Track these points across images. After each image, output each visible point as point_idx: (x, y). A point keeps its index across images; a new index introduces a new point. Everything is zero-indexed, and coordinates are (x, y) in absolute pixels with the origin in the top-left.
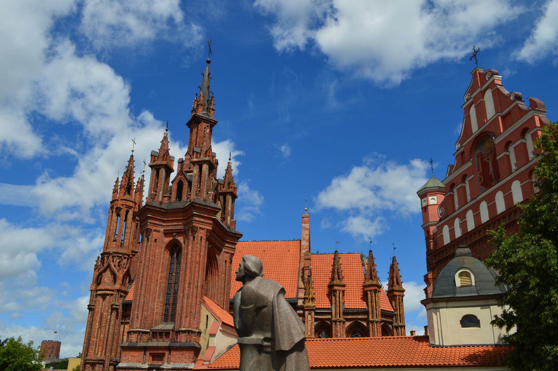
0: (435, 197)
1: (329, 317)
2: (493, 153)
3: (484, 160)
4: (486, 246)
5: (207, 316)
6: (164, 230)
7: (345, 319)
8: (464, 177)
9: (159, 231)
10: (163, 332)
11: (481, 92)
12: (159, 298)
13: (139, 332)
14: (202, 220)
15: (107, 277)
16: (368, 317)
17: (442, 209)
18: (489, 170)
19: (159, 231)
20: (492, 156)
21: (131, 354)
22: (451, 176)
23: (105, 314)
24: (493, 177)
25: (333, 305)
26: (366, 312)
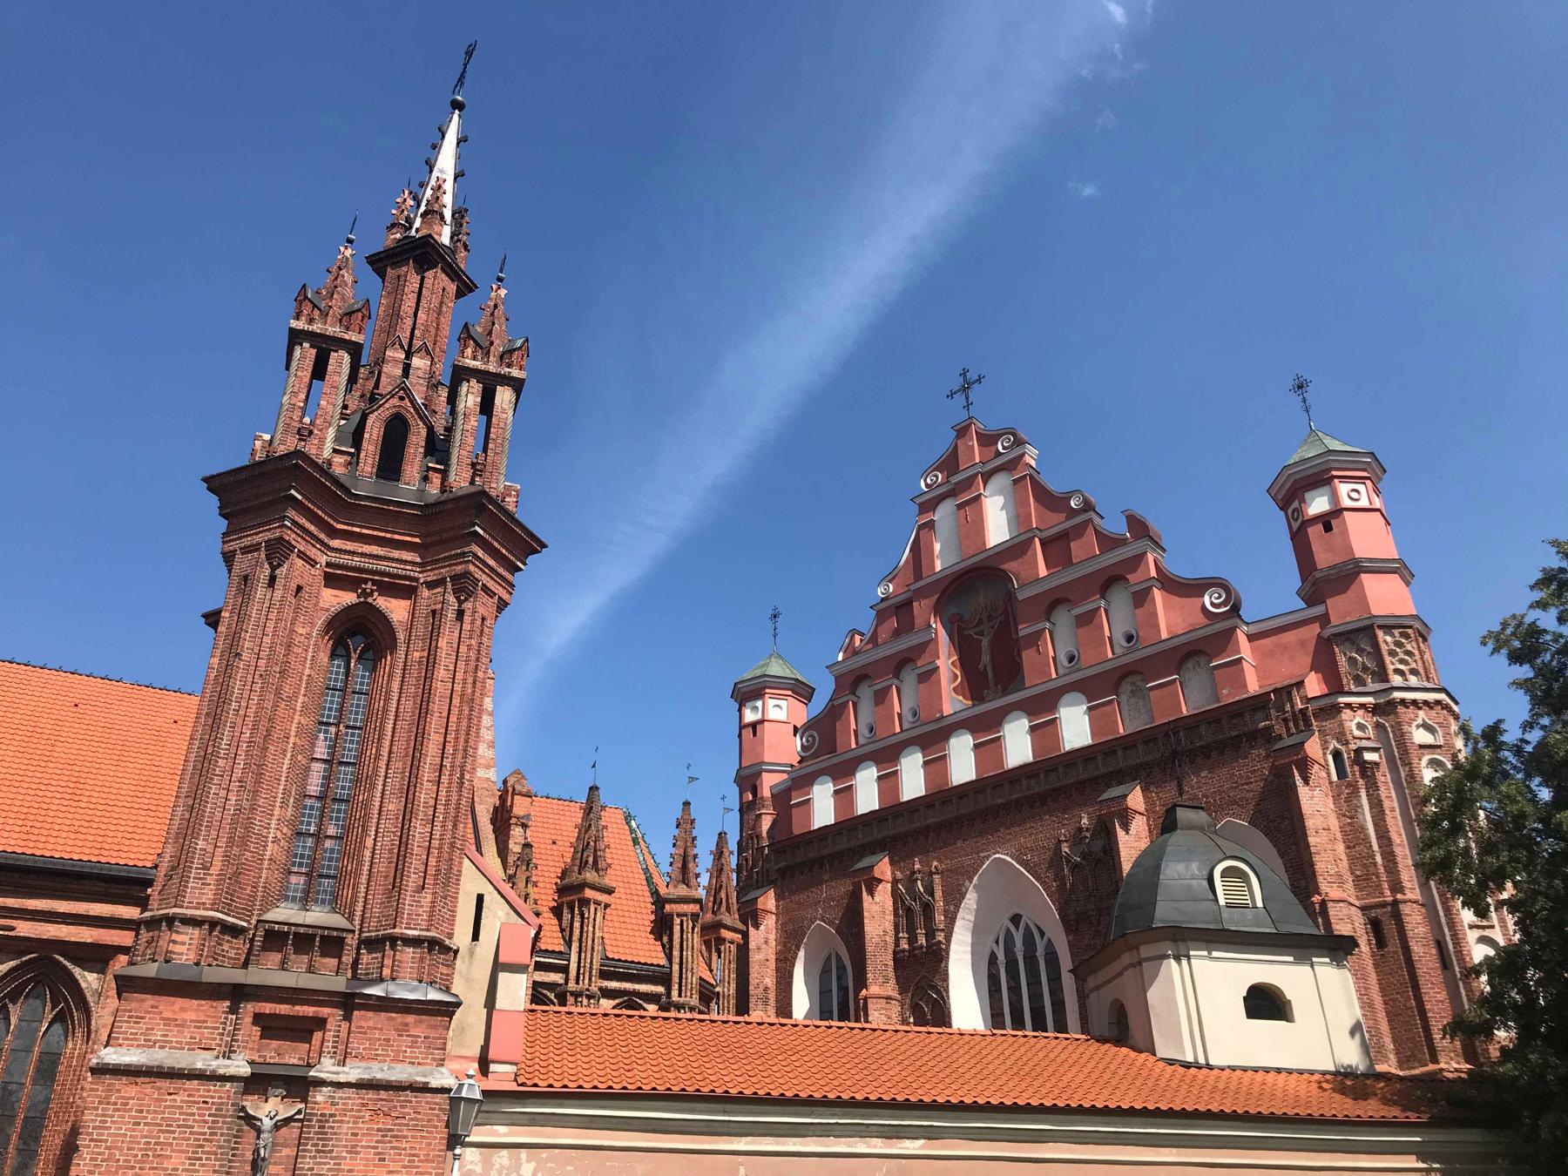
0: (783, 703)
1: (557, 978)
3: (966, 633)
5: (480, 898)
6: (328, 565)
7: (601, 989)
9: (312, 562)
10: (313, 936)
12: (284, 804)
13: (213, 923)
14: (491, 562)
16: (669, 994)
17: (812, 736)
19: (312, 562)
21: (166, 1015)
24: (990, 676)
25: (575, 946)
26: (664, 978)
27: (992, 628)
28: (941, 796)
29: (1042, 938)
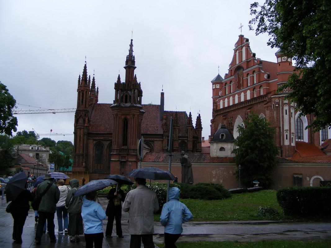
0: (219, 85)
8: (231, 82)
9: (120, 114)
11: (241, 47)
15: (81, 121)
19: (120, 114)
22: (226, 80)
23: (82, 136)
28: (234, 105)
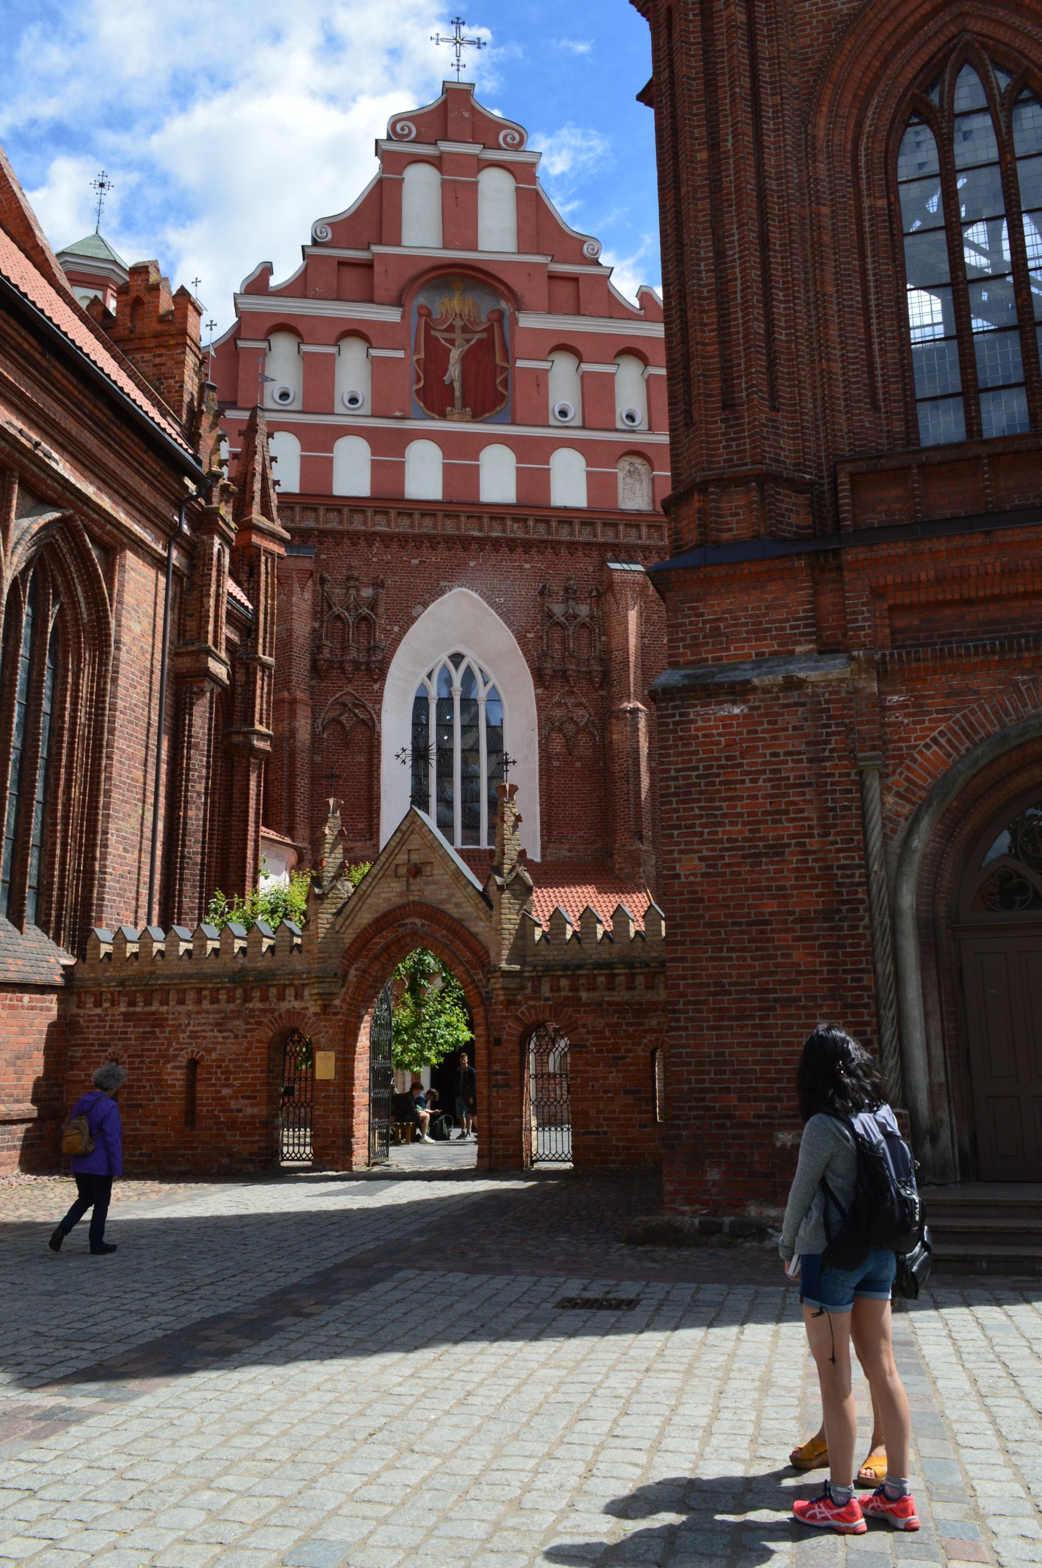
2: (477, 336)
3: (433, 332)
4: (415, 562)
18: (446, 370)
20: (468, 341)
24: (458, 394)
27: (468, 341)
29: (485, 684)
